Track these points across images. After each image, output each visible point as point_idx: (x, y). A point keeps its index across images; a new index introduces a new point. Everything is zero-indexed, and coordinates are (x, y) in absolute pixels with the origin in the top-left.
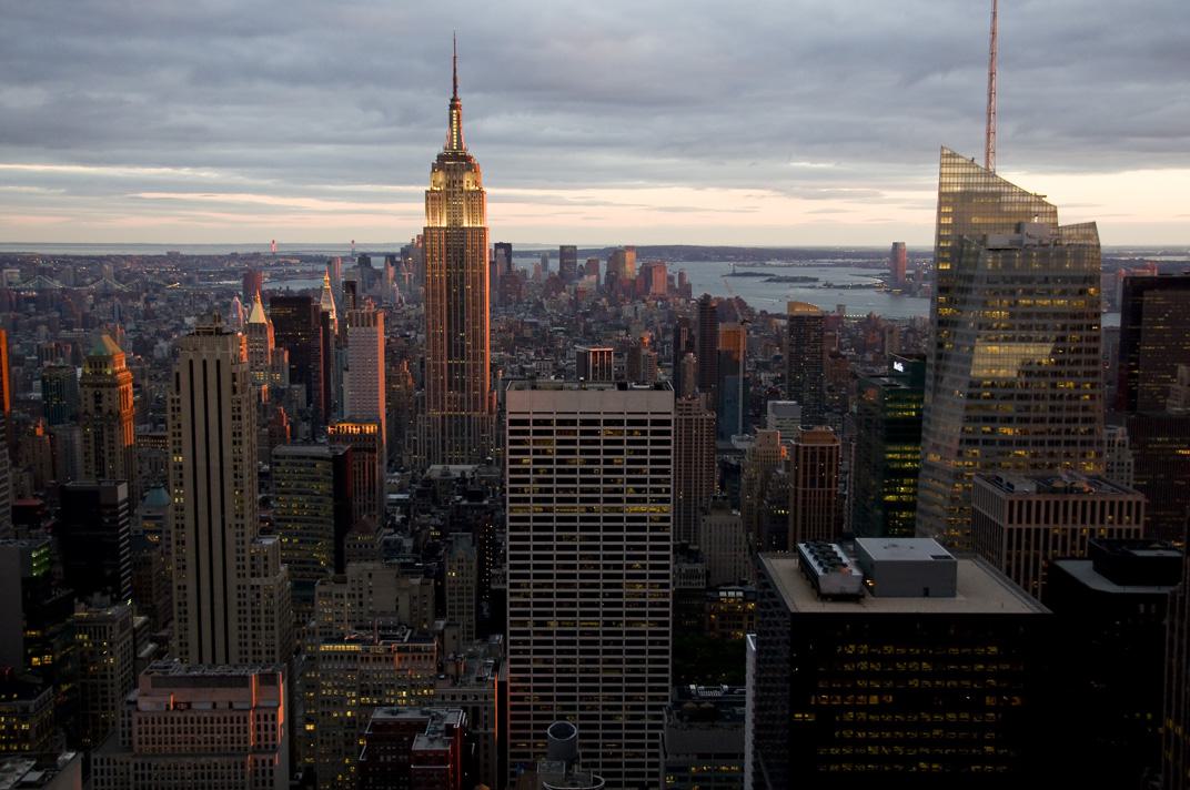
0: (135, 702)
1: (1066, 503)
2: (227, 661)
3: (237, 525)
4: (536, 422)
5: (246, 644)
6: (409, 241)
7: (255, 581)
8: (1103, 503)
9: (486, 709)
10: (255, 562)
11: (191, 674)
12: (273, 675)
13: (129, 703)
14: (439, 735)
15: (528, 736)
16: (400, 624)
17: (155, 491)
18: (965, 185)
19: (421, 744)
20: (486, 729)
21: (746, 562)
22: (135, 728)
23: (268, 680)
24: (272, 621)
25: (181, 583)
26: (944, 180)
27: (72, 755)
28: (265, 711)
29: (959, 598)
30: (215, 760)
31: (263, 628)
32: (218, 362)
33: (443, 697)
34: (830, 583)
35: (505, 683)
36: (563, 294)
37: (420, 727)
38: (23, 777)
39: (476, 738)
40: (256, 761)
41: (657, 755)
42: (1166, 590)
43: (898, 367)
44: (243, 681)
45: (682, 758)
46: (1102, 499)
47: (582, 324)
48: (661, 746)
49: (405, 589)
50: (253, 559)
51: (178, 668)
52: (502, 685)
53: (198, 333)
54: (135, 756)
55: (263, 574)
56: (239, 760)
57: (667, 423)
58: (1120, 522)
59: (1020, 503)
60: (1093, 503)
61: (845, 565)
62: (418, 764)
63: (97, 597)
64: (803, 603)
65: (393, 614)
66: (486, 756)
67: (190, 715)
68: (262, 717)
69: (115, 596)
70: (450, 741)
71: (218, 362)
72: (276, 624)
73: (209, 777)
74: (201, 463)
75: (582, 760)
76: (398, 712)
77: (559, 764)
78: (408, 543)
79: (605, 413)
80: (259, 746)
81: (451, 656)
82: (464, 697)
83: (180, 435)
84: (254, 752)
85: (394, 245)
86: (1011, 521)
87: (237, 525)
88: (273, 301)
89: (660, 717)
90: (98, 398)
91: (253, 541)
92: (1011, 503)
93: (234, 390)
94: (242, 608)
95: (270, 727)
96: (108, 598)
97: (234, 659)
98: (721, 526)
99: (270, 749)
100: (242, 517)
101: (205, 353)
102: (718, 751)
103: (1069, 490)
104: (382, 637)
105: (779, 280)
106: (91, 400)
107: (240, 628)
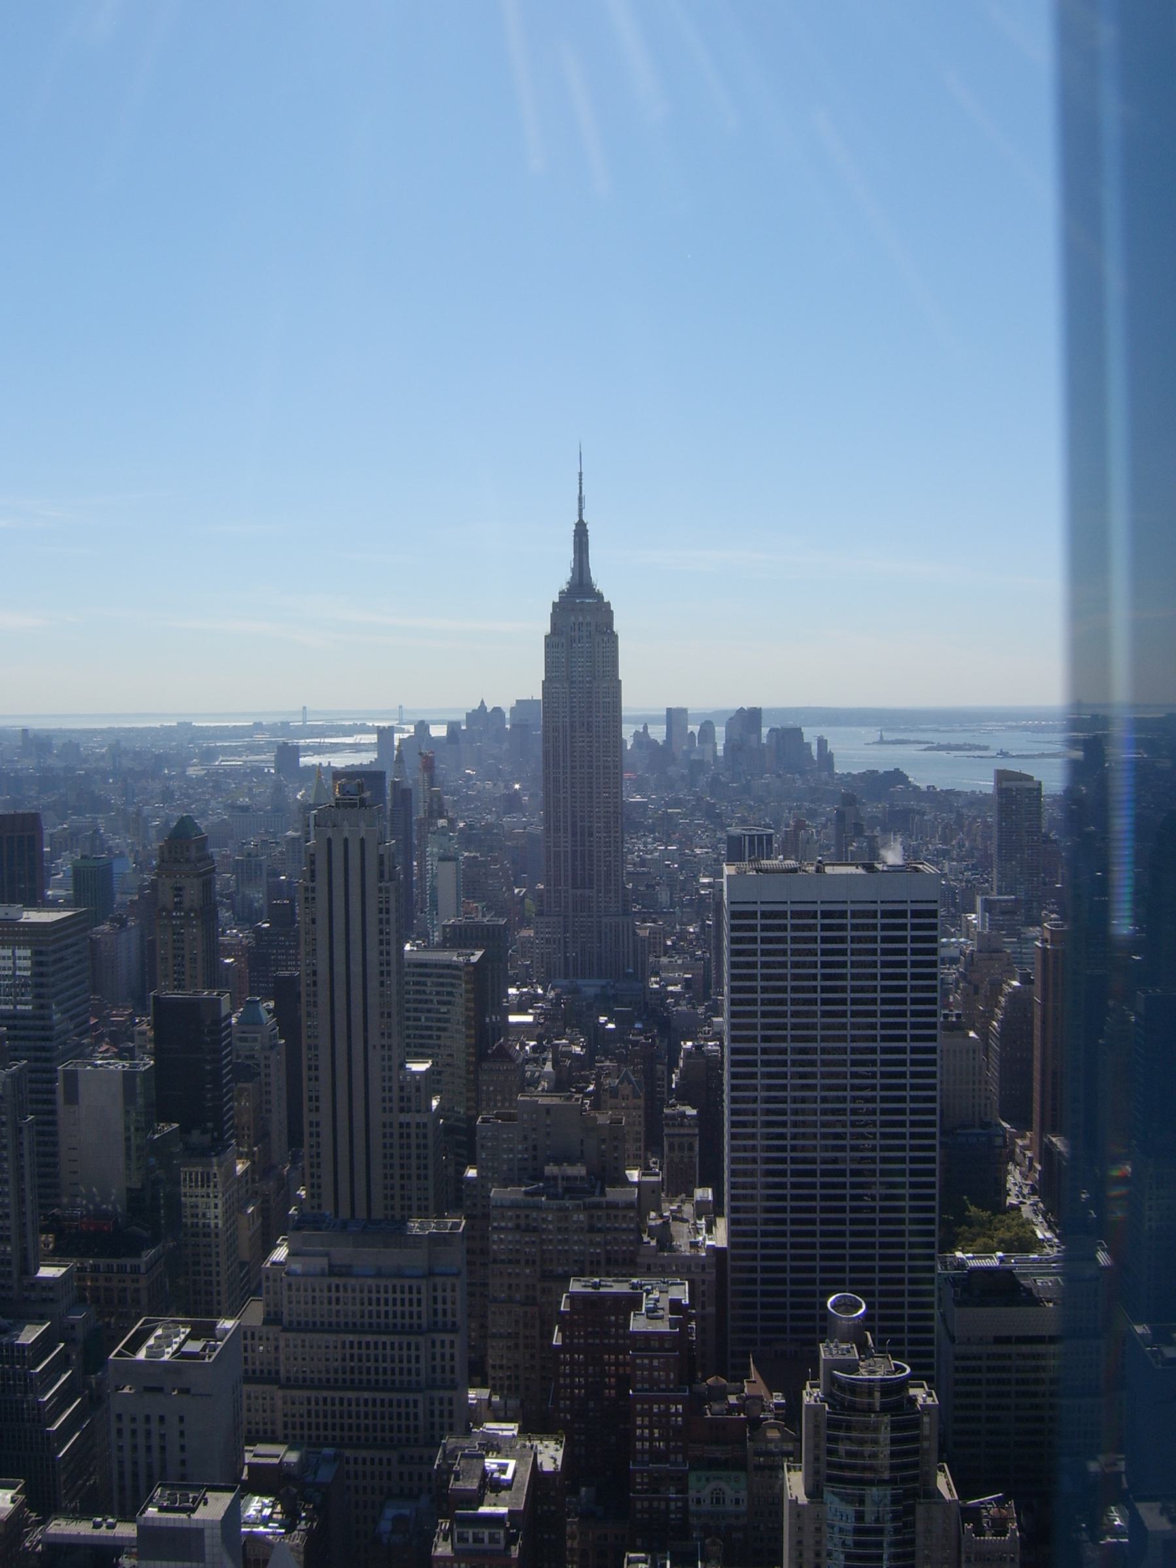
0: (281, 1263)
3: (383, 1046)
4: (765, 915)
5: (392, 1197)
7: (404, 1118)
13: (274, 1263)
19: (638, 1324)
20: (703, 1308)
22: (286, 1293)
24: (426, 1167)
30: (384, 1338)
31: (414, 1177)
32: (362, 840)
40: (433, 1343)
50: (402, 1089)
54: (285, 1330)
56: (413, 1339)
57: (933, 914)
63: (196, 1137)
69: (216, 1134)
71: (362, 840)
72: (430, 1172)
73: (376, 1360)
74: (340, 968)
77: (844, 1346)
79: (852, 902)
80: (436, 1323)
87: (383, 1046)
90: (178, 890)
96: (208, 1137)
98: (968, 1051)
100: (390, 1036)
102: (1021, 1334)
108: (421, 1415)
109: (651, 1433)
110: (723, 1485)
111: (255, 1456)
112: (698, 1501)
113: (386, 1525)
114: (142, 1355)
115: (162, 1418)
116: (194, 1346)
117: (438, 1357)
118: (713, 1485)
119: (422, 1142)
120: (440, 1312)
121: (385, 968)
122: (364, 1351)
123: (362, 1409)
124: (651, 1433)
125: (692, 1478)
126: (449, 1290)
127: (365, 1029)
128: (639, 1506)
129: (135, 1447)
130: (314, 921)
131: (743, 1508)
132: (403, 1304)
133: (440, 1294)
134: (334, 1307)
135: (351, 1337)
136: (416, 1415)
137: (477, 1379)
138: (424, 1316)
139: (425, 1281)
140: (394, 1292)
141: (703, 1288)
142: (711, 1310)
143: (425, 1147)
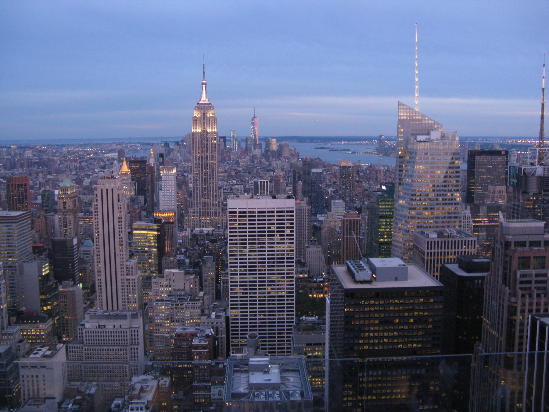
1: (448, 242)
2: (118, 309)
5: (125, 302)
6: (185, 136)
7: (128, 277)
8: (462, 241)
9: (221, 327)
10: (128, 269)
11: (105, 314)
12: (137, 314)
13: (81, 325)
14: (203, 338)
15: (238, 338)
16: (186, 294)
17: (87, 240)
18: (408, 116)
19: (196, 342)
20: (221, 335)
21: (324, 266)
22: (84, 334)
23: (134, 316)
25: (99, 278)
26: (400, 114)
27: (62, 345)
29: (409, 281)
30: (115, 347)
32: (112, 189)
33: (204, 323)
34: (360, 276)
35: (229, 317)
36: (247, 157)
37: (194, 335)
38: (45, 353)
39: (217, 339)
41: (290, 344)
42: (484, 274)
43: (384, 188)
44: (124, 317)
45: (301, 345)
46: (462, 239)
47: (255, 170)
48: (292, 341)
49: (187, 280)
50: (127, 268)
51: (100, 312)
52: (227, 318)
53: (104, 178)
54: (85, 346)
55: (131, 274)
56: (125, 348)
57: (293, 212)
58: (468, 248)
59: (431, 242)
60: (458, 241)
61: (365, 269)
62: (195, 349)
64: (349, 285)
65: (183, 290)
66: (222, 346)
68: (133, 331)
70: (208, 340)
71: (112, 189)
75: (261, 347)
76: (186, 329)
77: (252, 349)
78: (187, 261)
80: (132, 343)
81: (207, 307)
82: (212, 323)
83: (98, 219)
84: (130, 345)
85: (178, 137)
86: (428, 249)
88: (131, 162)
89: (291, 330)
91: (127, 261)
92: (428, 242)
93: (119, 201)
94: (123, 288)
95: (136, 335)
97: (121, 308)
99: (137, 343)
100: (122, 251)
101: (107, 186)
103: (449, 236)
104: (179, 299)
105: (335, 150)
106: (62, 205)
107: (123, 296)
108: (128, 371)
109: (199, 374)
110: (222, 389)
111: (71, 385)
113: (113, 406)
114: (32, 356)
117: (133, 353)
118: (219, 389)
119: (134, 285)
120: (133, 339)
121: (120, 230)
123: (109, 369)
124: (199, 374)
125: (212, 388)
126: (136, 332)
127: (115, 249)
130: (97, 215)
132: (121, 337)
133: (133, 333)
134: (100, 338)
135: (105, 348)
136: (126, 371)
138: (128, 340)
139: (128, 330)
140: (119, 333)
141: (221, 329)
142: (224, 336)
143: (135, 286)
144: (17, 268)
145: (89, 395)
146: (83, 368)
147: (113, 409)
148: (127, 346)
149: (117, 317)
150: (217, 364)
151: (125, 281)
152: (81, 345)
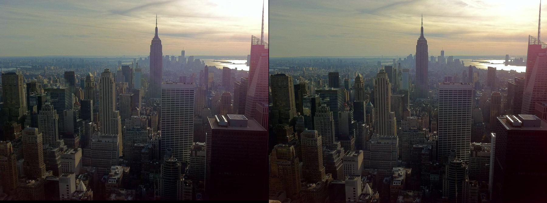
0: (371, 142)
13: (370, 142)
28: (394, 144)
44: (390, 139)
67: (381, 145)
104: (414, 131)
110: (435, 176)
112: (432, 179)
115: (351, 165)
116: (356, 154)
122: (382, 155)
125: (431, 175)
128: (423, 179)
129: (347, 169)
131: (438, 180)
133: (394, 147)
134: (378, 148)
135: (380, 153)
137: (400, 159)
141: (434, 146)
142: (435, 150)
144: (339, 115)
145: (374, 175)
146: (370, 162)
147: (384, 183)
148: (391, 152)
149: (386, 139)
150: (433, 163)
151: (389, 122)
152: (369, 151)
